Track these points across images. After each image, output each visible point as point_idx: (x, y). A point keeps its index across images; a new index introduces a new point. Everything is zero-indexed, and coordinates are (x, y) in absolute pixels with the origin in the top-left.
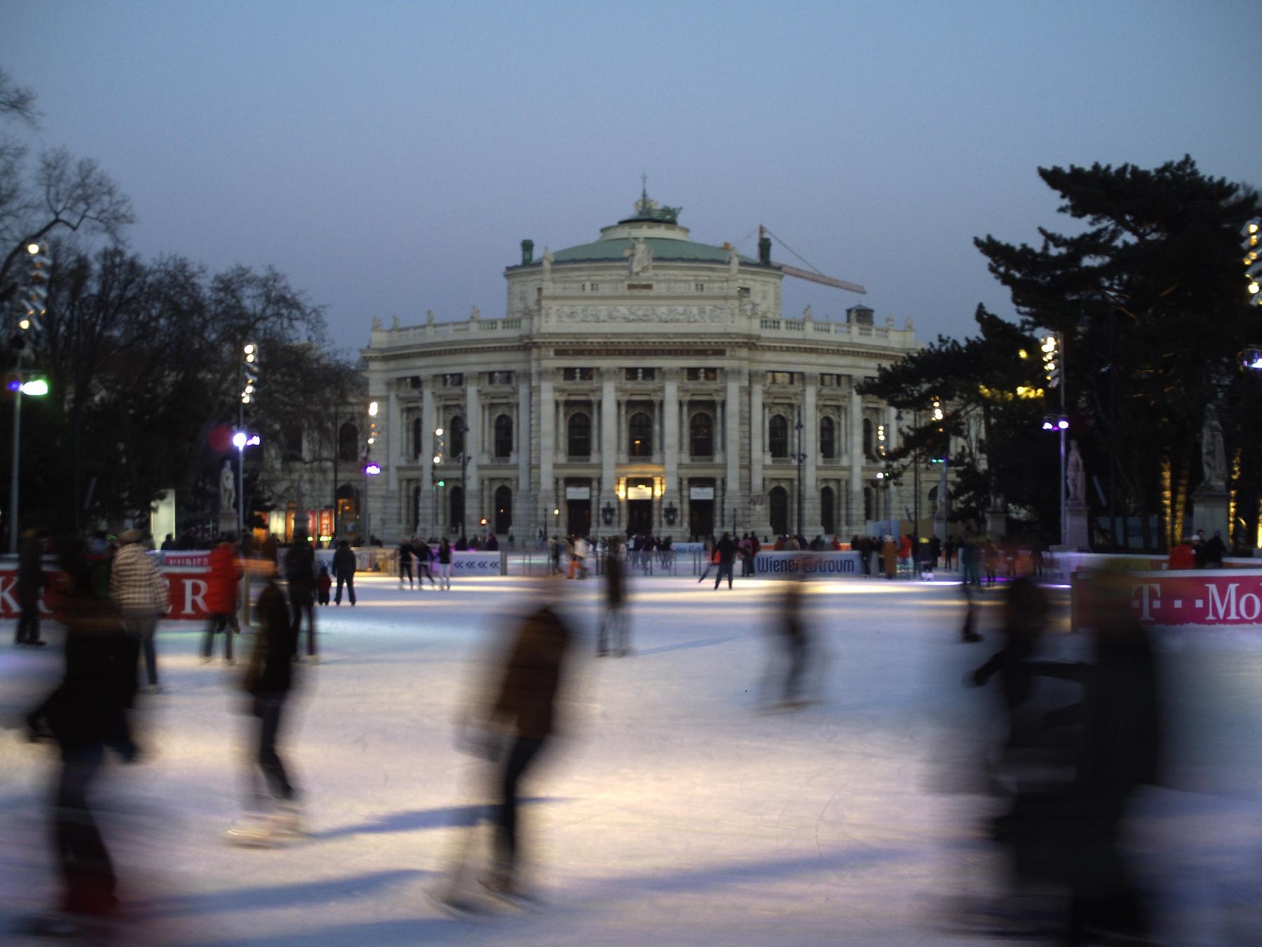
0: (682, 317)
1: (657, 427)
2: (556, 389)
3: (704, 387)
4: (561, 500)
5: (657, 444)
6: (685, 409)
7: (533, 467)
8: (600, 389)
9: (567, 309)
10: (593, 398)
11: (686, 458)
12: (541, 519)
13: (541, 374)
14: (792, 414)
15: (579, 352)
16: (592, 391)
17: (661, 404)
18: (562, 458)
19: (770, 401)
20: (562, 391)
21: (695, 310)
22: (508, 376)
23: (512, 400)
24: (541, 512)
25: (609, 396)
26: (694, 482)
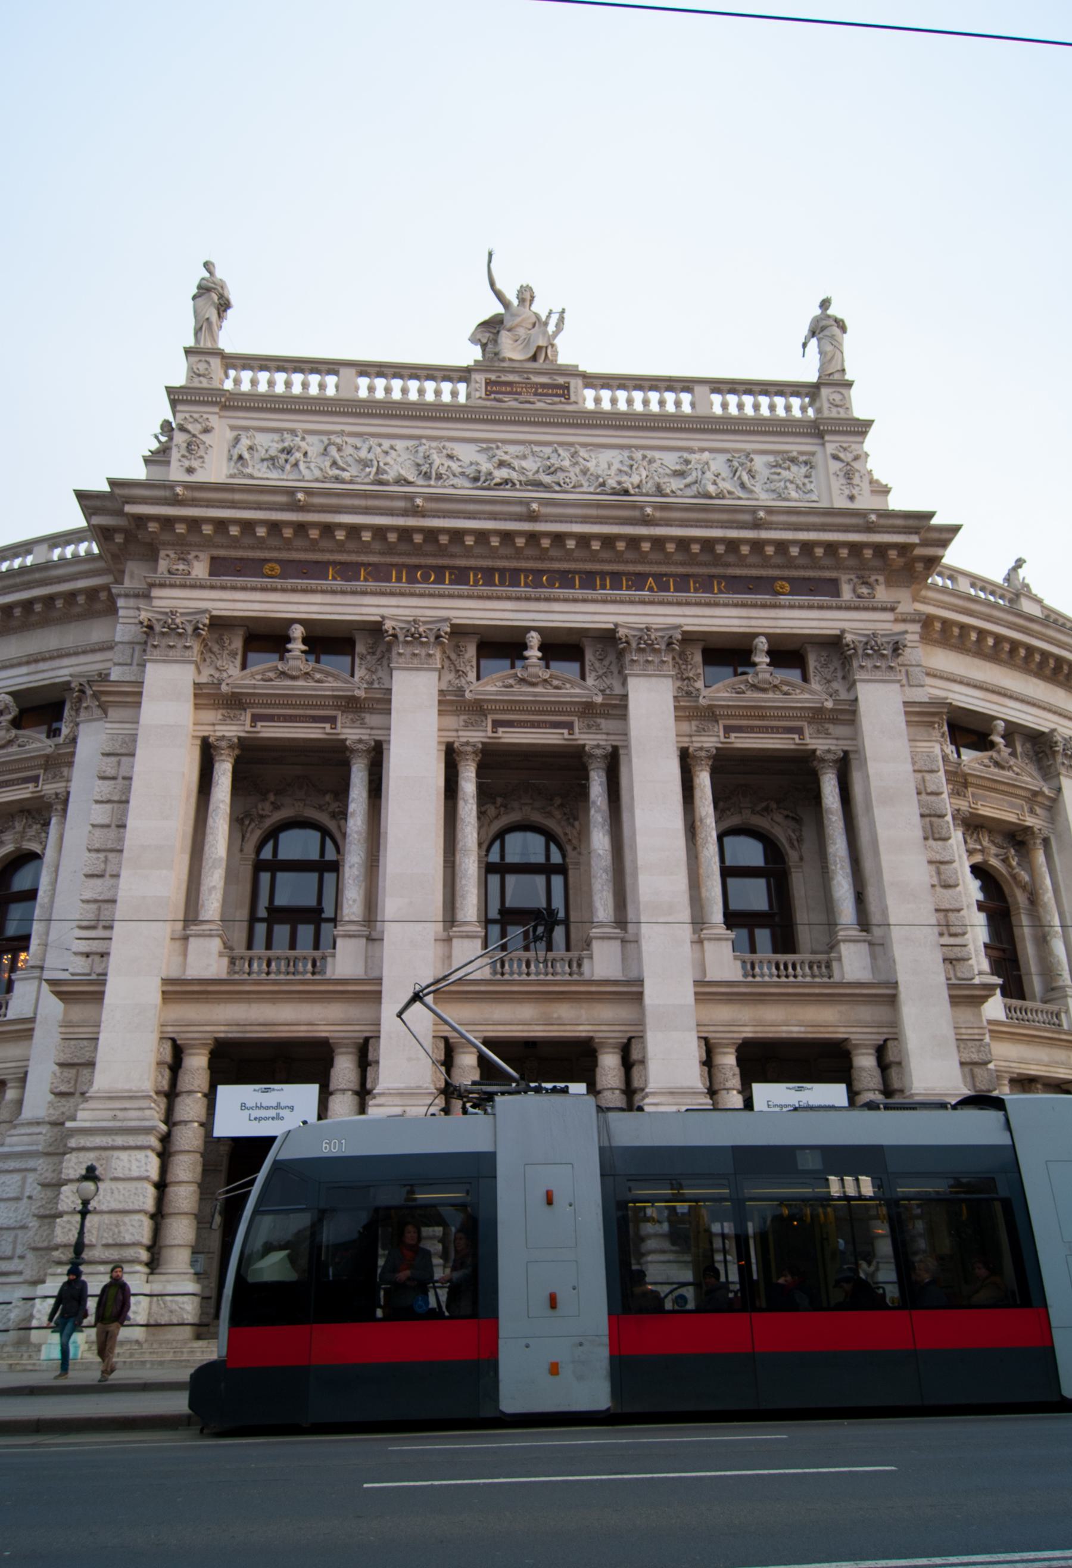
0: (676, 484)
1: (600, 841)
2: (207, 696)
3: (771, 698)
4: (189, 1138)
5: (603, 908)
6: (704, 780)
7: (85, 993)
8: (383, 704)
9: (268, 443)
10: (350, 733)
11: (724, 962)
12: (65, 1231)
13: (155, 636)
14: (1032, 870)
15: (305, 571)
16: (352, 705)
17: (613, 763)
18: (207, 960)
19: (963, 805)
20: (234, 703)
21: (718, 464)
22: (42, 709)
23: (49, 788)
24: (69, 1198)
25: (415, 728)
26: (765, 1060)
